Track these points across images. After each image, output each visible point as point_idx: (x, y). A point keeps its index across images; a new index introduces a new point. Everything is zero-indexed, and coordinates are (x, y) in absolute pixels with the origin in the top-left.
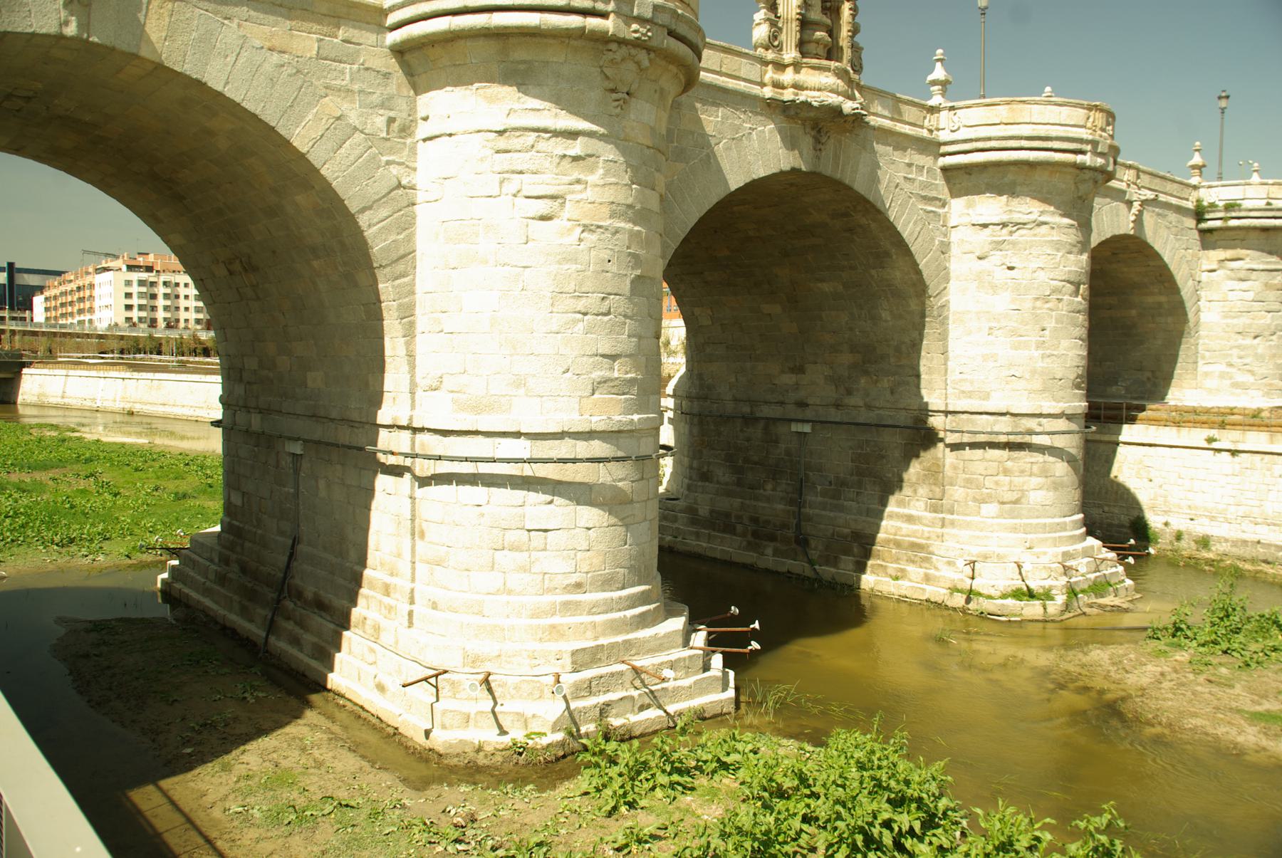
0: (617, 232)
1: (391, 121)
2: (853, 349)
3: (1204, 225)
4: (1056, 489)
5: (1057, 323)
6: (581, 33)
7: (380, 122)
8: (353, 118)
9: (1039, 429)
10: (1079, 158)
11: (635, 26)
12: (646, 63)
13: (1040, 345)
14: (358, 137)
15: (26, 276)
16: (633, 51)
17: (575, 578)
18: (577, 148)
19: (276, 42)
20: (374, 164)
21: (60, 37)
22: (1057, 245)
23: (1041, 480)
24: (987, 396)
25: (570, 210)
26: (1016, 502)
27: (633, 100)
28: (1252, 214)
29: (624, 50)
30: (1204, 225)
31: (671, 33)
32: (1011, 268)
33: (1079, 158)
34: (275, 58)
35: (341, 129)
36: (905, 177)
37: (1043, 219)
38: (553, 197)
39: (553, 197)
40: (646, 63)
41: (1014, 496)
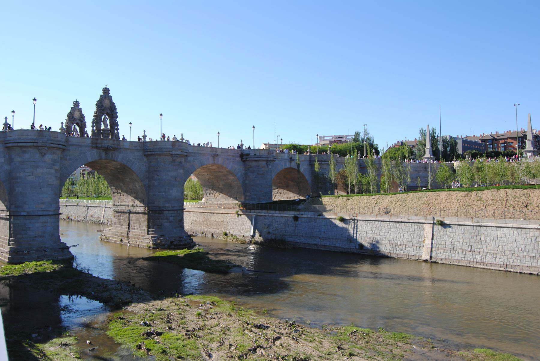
2: (134, 193)
3: (243, 160)
9: (165, 210)
10: (171, 153)
12: (47, 149)
16: (44, 148)
17: (35, 236)
23: (166, 221)
24: (154, 203)
26: (161, 225)
27: (46, 155)
29: (42, 148)
30: (243, 160)
31: (51, 144)
32: (158, 176)
40: (47, 149)
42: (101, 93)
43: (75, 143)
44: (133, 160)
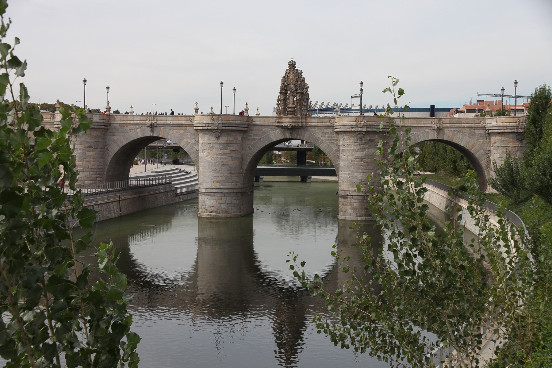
0: (218, 157)
1: (195, 141)
4: (354, 209)
5: (353, 169)
6: (207, 129)
7: (194, 141)
8: (189, 141)
9: (349, 194)
11: (215, 127)
13: (349, 174)
14: (190, 144)
15: (425, 117)
17: (211, 211)
18: (211, 145)
19: (178, 132)
20: (193, 147)
21: (150, 136)
22: (353, 150)
23: (350, 207)
25: (210, 155)
26: (345, 212)
28: (493, 128)
33: (353, 129)
34: (177, 134)
35: (188, 143)
36: (321, 136)
37: (349, 144)
38: (208, 153)
39: (208, 153)
41: (345, 210)
42: (287, 67)
43: (259, 123)
44: (322, 138)
